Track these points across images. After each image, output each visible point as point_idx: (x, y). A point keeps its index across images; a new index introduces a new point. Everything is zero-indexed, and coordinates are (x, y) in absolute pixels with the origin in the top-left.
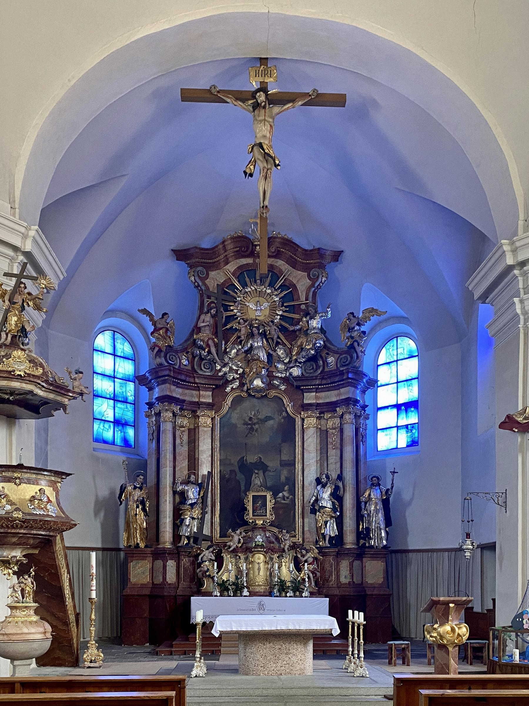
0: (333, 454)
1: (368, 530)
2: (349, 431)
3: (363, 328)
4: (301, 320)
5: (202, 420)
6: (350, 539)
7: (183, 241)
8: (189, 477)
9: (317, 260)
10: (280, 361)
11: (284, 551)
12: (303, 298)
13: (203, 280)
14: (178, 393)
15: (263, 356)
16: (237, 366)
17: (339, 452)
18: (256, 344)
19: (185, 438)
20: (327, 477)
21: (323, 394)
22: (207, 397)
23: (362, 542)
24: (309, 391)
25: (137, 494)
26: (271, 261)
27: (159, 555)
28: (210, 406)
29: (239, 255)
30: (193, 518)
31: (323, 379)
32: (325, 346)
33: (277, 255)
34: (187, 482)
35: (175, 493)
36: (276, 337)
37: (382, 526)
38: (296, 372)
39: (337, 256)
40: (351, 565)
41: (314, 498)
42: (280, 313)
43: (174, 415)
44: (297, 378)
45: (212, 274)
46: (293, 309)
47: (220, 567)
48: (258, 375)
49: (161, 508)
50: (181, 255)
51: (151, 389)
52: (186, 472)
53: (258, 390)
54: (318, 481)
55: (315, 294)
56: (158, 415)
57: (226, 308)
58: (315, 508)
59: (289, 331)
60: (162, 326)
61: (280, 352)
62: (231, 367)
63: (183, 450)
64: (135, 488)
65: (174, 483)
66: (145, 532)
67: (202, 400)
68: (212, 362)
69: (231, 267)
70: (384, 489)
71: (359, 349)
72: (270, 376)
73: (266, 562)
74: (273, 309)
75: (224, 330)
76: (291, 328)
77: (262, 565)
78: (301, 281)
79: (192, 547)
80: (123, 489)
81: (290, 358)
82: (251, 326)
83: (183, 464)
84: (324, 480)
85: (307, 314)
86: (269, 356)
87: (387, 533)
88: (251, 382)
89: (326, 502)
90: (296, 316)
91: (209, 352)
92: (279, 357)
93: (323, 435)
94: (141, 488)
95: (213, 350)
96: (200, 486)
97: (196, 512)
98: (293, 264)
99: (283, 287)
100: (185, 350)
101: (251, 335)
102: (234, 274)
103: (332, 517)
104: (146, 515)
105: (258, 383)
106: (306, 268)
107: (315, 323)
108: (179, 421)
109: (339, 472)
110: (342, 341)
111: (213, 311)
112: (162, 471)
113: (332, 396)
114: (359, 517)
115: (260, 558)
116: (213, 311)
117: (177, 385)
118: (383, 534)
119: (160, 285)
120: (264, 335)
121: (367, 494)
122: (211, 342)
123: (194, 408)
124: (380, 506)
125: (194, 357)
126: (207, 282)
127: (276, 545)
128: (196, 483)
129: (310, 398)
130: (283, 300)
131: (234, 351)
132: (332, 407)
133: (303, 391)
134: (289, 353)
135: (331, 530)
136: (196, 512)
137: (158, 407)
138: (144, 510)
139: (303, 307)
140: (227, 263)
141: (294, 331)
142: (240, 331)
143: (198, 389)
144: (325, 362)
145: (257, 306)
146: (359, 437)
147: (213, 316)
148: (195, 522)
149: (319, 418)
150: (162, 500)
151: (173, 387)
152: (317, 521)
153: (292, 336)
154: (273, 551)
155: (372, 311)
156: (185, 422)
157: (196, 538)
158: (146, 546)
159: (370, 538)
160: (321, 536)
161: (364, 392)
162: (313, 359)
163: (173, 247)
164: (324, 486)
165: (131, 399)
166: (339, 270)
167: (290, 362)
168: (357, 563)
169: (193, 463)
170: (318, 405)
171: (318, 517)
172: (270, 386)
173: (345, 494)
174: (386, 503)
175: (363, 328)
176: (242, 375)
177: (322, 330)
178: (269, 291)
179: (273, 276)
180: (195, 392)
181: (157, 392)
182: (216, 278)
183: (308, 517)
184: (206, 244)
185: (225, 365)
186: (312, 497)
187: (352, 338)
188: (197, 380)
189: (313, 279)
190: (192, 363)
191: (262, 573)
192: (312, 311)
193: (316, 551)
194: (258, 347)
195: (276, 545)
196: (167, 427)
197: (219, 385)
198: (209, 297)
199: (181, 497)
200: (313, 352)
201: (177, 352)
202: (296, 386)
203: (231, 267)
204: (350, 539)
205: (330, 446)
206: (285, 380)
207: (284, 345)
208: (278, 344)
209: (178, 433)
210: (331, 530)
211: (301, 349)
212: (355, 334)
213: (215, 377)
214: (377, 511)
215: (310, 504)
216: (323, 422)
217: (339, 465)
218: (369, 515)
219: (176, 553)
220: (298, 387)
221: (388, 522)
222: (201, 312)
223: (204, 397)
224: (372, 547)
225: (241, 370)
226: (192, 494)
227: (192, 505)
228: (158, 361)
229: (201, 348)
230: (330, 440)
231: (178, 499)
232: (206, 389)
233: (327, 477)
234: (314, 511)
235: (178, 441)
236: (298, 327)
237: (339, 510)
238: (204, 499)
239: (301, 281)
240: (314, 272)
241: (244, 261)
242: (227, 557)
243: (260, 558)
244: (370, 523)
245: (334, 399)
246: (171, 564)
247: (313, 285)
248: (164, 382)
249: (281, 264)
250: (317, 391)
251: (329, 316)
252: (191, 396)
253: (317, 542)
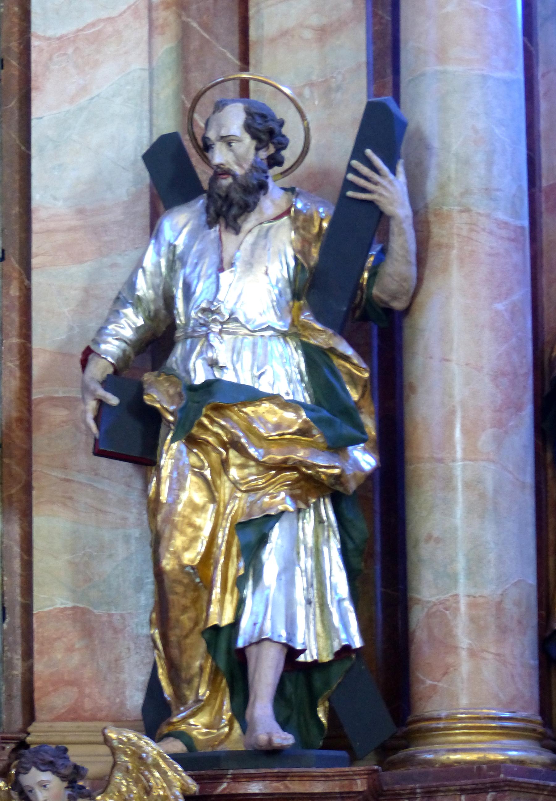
20: (266, 130)
41: (129, 323)
54: (171, 171)
58: (144, 411)
84: (234, 153)
103: (309, 487)
135: (298, 598)
152: (157, 522)
160: (198, 659)
164: (229, 207)
171: (178, 484)
173: (431, 284)
183: (67, 500)
186: (115, 313)
210: (298, 598)
215: (99, 369)
217: (353, 48)
233: (266, 130)
234: (132, 433)
237: (370, 426)
253: (156, 715)
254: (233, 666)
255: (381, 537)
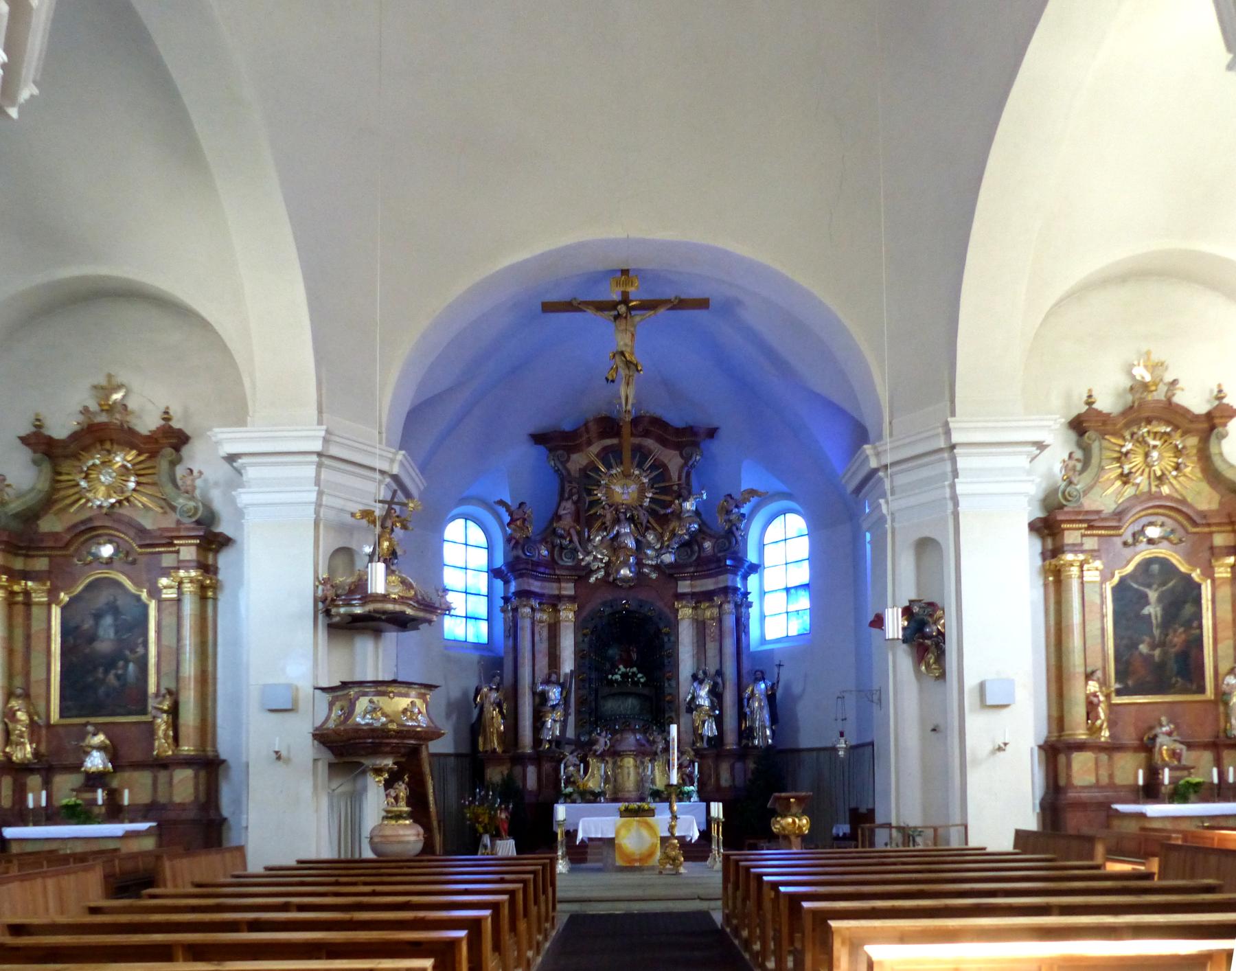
0: (712, 648)
1: (751, 729)
2: (729, 622)
3: (743, 511)
4: (672, 502)
5: (563, 614)
6: (731, 741)
7: (540, 423)
8: (550, 676)
9: (690, 438)
10: (650, 546)
11: (656, 754)
12: (675, 477)
13: (564, 463)
14: (536, 586)
15: (630, 543)
16: (602, 554)
17: (717, 644)
18: (623, 531)
19: (545, 633)
20: (705, 673)
21: (698, 582)
22: (568, 589)
23: (744, 742)
24: (684, 579)
25: (494, 695)
26: (637, 441)
27: (519, 760)
28: (572, 599)
29: (603, 435)
30: (555, 721)
31: (698, 565)
32: (700, 530)
33: (646, 434)
34: (548, 682)
35: (534, 693)
36: (644, 522)
37: (768, 723)
38: (668, 558)
39: (712, 433)
40: (732, 768)
42: (650, 495)
43: (533, 609)
44: (670, 565)
45: (574, 457)
46: (665, 490)
47: (586, 772)
48: (625, 564)
49: (520, 710)
50: (539, 438)
51: (506, 582)
52: (546, 671)
53: (625, 579)
54: (695, 677)
55: (688, 475)
56: (515, 610)
57: (589, 492)
58: (692, 707)
59: (660, 515)
60: (517, 516)
61: (651, 537)
62: (596, 556)
63: (543, 647)
64: (491, 689)
65: (534, 683)
66: (502, 737)
67: (564, 593)
68: (575, 551)
69: (595, 449)
70: (769, 683)
71: (738, 534)
72: (639, 564)
73: (636, 767)
74: (642, 492)
75: (587, 517)
76: (662, 512)
77: (632, 770)
78: (673, 460)
79: (554, 752)
80: (478, 691)
81: (662, 544)
82: (617, 510)
83: (543, 663)
84: (701, 675)
85: (679, 496)
86: (638, 542)
87: (773, 732)
88: (618, 572)
89: (704, 701)
90: (668, 498)
91: (571, 541)
92: (649, 543)
93: (701, 627)
94: (497, 690)
95: (575, 539)
96: (562, 686)
97: (558, 715)
98: (664, 442)
99: (653, 467)
100: (544, 541)
101: (617, 521)
102: (597, 455)
103: (710, 716)
104: (503, 717)
105: (625, 572)
106: (679, 447)
107: (689, 506)
108: (538, 616)
109: (718, 667)
110: (720, 523)
111: (575, 498)
112: (521, 671)
113: (709, 584)
114: (742, 716)
115: (629, 762)
116: (575, 498)
117: (536, 578)
118: (768, 732)
119: (516, 470)
120: (631, 520)
121: (749, 691)
122: (572, 531)
123: (554, 602)
124: (764, 703)
125: (554, 547)
126: (569, 465)
127: (648, 748)
128: (558, 683)
129: (684, 587)
130: (653, 481)
131: (598, 538)
132: (708, 596)
133: (677, 580)
134: (660, 537)
135: (709, 729)
136: (558, 715)
137: (515, 601)
138: (501, 712)
139: (676, 488)
140: (589, 443)
141: (666, 515)
142: (605, 516)
143: (559, 581)
144: (701, 547)
145: (624, 490)
146: (741, 626)
147: (575, 503)
148: (558, 725)
149: (695, 608)
150: (520, 702)
151: (531, 581)
152: (693, 721)
153: (663, 520)
154: (644, 754)
155: (752, 492)
156: (545, 617)
157: (558, 742)
158: (504, 752)
159: (754, 738)
161: (745, 578)
162: (685, 545)
163: (532, 430)
164: (701, 682)
165: (485, 591)
166: (715, 447)
167: (661, 548)
168: (738, 765)
169: (554, 660)
170: (693, 595)
172: (639, 575)
174: (771, 698)
175: (743, 511)
176: (608, 564)
177: (697, 513)
178: (637, 472)
179: (641, 455)
180: (555, 585)
181: (513, 587)
182: (578, 461)
184: (567, 426)
185: (588, 553)
187: (730, 521)
188: (557, 572)
189: (687, 459)
190: (551, 553)
191: (632, 777)
192: (685, 492)
193: (692, 753)
194: (626, 534)
195: (648, 748)
196: (526, 624)
197: (581, 574)
198: (570, 482)
199: (541, 699)
200: (687, 537)
201: (535, 542)
202: (670, 574)
203: (595, 449)
204: (731, 741)
205: (708, 639)
206: (656, 568)
207: (654, 529)
208: (647, 529)
209: (537, 629)
210: (709, 729)
211: (673, 534)
212: (733, 517)
213: (577, 567)
214: (761, 707)
216: (699, 612)
217: (718, 659)
218: (752, 712)
219: (537, 758)
220: (671, 575)
221: (774, 719)
222: (562, 498)
223: (565, 589)
224: (755, 747)
225: (606, 559)
226: (554, 694)
227: (554, 707)
228: (515, 553)
229: (562, 537)
230: (707, 631)
231: (537, 700)
232: (568, 581)
233: (705, 673)
235: (537, 638)
236: (669, 511)
238: (566, 700)
239: (673, 460)
240: (687, 450)
241: (608, 442)
242: (592, 761)
243: (629, 762)
244: (753, 721)
245: (712, 587)
246: (531, 771)
247: (686, 464)
248: (521, 576)
249: (650, 443)
250: (692, 578)
251: (705, 497)
252: (551, 589)
253: (694, 743)
254: (701, 737)
255: (719, 721)
